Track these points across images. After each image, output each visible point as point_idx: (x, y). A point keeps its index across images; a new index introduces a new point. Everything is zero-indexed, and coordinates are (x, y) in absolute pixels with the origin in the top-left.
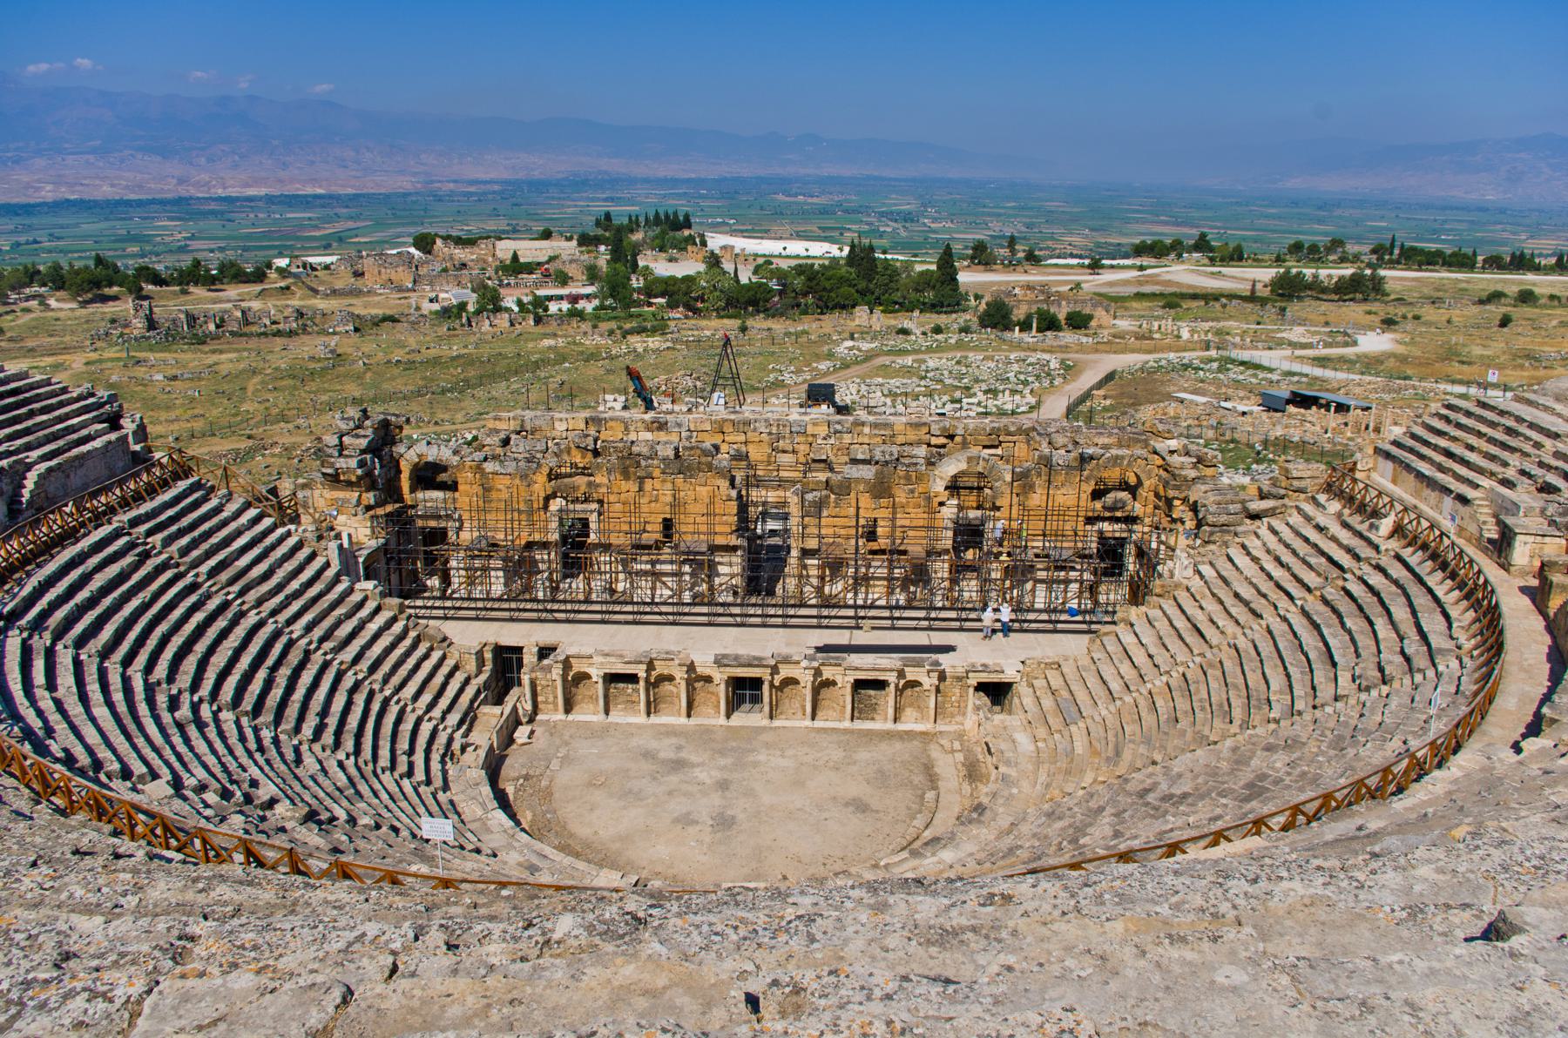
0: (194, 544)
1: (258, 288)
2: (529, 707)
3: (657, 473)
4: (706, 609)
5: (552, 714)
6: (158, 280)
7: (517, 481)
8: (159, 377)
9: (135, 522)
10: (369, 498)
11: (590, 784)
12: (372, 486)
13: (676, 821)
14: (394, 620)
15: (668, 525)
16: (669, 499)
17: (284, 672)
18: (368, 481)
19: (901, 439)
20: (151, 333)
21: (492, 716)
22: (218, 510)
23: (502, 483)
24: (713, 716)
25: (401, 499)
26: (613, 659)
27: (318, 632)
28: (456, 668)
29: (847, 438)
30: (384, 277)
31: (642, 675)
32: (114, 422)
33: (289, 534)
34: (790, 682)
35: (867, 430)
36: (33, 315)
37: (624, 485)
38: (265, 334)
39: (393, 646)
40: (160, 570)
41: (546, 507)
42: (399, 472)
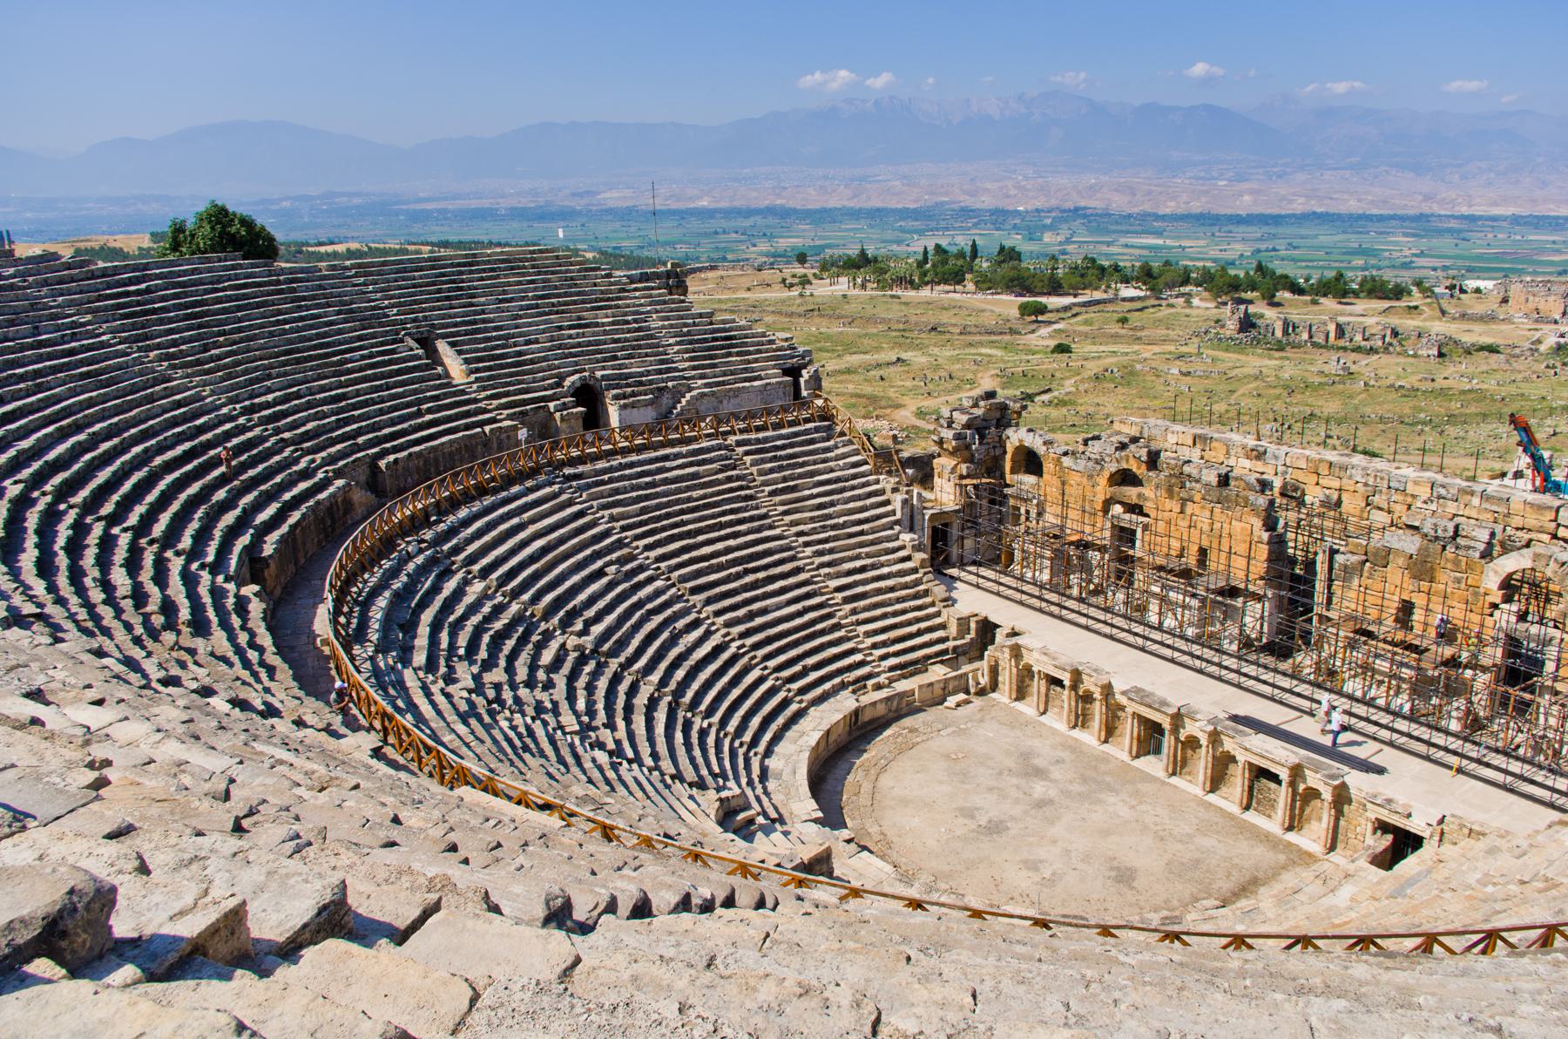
0: (781, 469)
1: (1386, 304)
2: (984, 680)
3: (1197, 498)
4: (1200, 649)
5: (1002, 697)
6: (1297, 290)
7: (1085, 480)
8: (1175, 371)
9: (739, 444)
10: (964, 468)
11: (948, 756)
12: (970, 460)
13: (961, 809)
14: (915, 571)
15: (1203, 552)
16: (1206, 528)
17: (761, 575)
18: (962, 450)
19: (1516, 521)
20: (1242, 335)
21: (938, 672)
22: (828, 450)
23: (1074, 479)
24: (1121, 750)
25: (1003, 476)
26: (1045, 658)
27: (826, 558)
28: (943, 626)
29: (1451, 508)
30: (1531, 305)
31: (1067, 683)
32: (794, 372)
33: (877, 482)
34: (1192, 743)
35: (1476, 501)
36: (1172, 310)
37: (1169, 504)
38: (1345, 349)
39: (892, 589)
40: (738, 478)
41: (1106, 510)
42: (1005, 452)
